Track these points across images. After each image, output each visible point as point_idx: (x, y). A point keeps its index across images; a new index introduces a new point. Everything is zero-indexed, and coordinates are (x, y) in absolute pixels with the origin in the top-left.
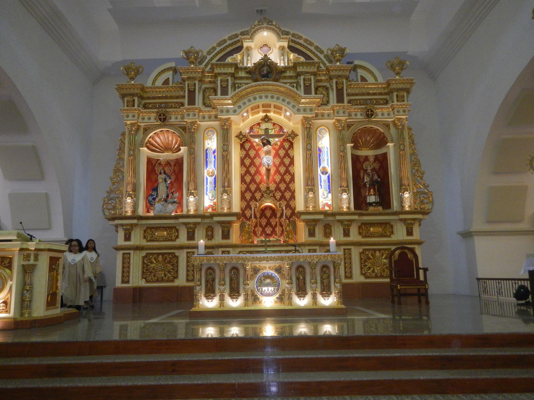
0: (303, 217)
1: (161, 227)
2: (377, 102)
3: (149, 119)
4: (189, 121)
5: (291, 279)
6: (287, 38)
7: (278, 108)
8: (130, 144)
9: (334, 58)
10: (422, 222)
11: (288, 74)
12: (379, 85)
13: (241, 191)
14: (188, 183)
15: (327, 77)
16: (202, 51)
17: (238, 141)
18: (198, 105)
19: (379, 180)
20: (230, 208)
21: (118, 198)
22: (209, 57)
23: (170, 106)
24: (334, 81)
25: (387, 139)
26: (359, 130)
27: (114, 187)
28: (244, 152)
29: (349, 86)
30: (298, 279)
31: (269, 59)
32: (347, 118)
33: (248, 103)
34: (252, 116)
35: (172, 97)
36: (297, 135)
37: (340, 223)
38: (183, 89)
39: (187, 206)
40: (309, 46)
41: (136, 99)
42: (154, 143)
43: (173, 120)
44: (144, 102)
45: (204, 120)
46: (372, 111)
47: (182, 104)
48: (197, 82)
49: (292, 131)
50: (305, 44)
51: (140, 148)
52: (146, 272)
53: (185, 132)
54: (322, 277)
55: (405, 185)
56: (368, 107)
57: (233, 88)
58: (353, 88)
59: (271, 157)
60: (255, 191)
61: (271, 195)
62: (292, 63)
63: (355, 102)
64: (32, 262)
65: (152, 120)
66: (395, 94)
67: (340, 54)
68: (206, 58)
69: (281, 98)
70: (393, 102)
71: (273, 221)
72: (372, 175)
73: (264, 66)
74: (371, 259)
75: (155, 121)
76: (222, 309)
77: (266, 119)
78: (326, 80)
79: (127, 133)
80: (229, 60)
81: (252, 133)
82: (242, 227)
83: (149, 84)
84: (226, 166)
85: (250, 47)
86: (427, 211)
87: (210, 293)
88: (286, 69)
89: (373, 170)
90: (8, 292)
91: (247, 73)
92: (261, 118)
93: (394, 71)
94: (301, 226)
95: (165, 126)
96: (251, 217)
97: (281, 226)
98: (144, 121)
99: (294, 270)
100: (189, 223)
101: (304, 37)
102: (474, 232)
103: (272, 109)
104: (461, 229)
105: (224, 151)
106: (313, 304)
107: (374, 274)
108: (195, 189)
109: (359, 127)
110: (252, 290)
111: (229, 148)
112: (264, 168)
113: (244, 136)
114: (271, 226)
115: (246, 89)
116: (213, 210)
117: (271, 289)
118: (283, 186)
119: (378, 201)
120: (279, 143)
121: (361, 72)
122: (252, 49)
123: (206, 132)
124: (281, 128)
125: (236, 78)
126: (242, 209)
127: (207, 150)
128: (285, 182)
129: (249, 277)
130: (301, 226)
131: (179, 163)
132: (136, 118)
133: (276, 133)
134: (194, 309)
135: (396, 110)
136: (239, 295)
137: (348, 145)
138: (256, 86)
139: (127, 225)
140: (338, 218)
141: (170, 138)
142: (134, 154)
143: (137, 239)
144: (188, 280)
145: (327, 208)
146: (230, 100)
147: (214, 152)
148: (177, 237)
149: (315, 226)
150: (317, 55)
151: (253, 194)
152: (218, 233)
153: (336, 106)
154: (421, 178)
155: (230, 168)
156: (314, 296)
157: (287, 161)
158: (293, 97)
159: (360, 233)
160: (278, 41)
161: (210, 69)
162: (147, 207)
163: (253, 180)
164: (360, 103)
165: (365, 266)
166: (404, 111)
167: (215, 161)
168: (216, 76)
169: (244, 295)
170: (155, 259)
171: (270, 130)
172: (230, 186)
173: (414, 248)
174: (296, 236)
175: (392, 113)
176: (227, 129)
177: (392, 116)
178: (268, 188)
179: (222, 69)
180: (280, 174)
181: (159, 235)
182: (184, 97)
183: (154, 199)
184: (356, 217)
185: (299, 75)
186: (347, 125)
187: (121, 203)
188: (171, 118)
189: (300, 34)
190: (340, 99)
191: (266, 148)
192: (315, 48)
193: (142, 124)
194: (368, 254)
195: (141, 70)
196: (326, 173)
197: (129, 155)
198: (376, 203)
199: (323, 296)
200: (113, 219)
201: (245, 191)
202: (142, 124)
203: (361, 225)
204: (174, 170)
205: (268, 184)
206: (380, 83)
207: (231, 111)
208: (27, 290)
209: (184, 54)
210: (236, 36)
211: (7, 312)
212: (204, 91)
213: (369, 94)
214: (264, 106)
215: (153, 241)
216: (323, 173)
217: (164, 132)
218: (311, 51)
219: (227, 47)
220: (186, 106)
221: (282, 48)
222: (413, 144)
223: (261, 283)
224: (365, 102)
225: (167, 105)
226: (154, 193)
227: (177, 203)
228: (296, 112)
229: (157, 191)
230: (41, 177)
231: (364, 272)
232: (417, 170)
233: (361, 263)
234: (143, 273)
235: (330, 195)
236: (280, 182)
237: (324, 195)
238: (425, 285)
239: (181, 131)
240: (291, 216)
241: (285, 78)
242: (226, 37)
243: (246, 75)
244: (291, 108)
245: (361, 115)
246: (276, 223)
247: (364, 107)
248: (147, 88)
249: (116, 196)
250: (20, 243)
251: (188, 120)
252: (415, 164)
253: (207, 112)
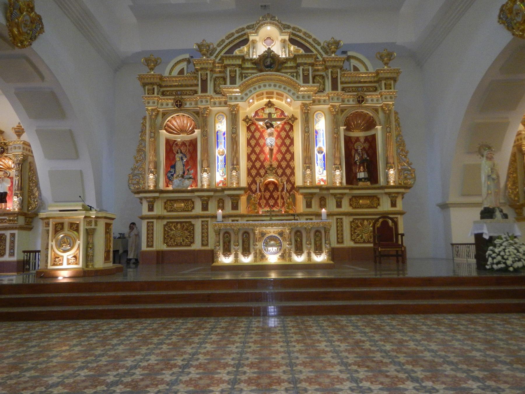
0: (301, 191)
1: (179, 200)
2: (367, 89)
3: (167, 105)
4: (203, 107)
5: (291, 241)
6: (288, 32)
7: (280, 96)
8: (151, 126)
9: (330, 49)
10: (405, 196)
11: (289, 64)
12: (369, 74)
13: (248, 168)
14: (202, 161)
15: (323, 67)
16: (212, 44)
17: (244, 123)
18: (210, 93)
19: (368, 158)
20: (238, 183)
21: (141, 174)
22: (219, 49)
23: (185, 93)
24: (330, 70)
25: (375, 122)
26: (351, 114)
27: (139, 164)
28: (250, 134)
29: (343, 76)
30: (296, 241)
31: (273, 51)
32: (341, 104)
33: (253, 91)
34: (257, 101)
35: (187, 86)
36: (297, 119)
37: (333, 196)
38: (196, 78)
39: (202, 182)
40: (308, 39)
41: (156, 87)
42: (171, 125)
43: (188, 105)
44: (162, 89)
45: (215, 106)
46: (362, 97)
47: (196, 92)
48: (208, 72)
49: (293, 115)
50: (304, 37)
51: (160, 131)
52: (167, 238)
53: (199, 117)
54: (315, 240)
55: (390, 163)
56: (360, 94)
57: (240, 77)
58: (346, 76)
59: (273, 139)
60: (260, 168)
61: (274, 171)
62: (292, 54)
63: (348, 89)
64: (93, 227)
65: (170, 106)
66: (383, 82)
67: (336, 47)
68: (216, 50)
69: (283, 86)
70: (381, 89)
71: (275, 195)
72: (362, 154)
73: (267, 57)
74: (360, 227)
75: (173, 107)
76: (236, 264)
77: (270, 104)
78: (322, 70)
79: (148, 118)
80: (237, 52)
81: (257, 117)
82: (249, 199)
83: (166, 74)
84: (235, 147)
85: (256, 40)
86: (409, 186)
87: (227, 251)
88: (287, 60)
89: (364, 149)
90: (77, 249)
91: (253, 63)
92: (265, 103)
93: (383, 61)
94: (300, 199)
95: (181, 111)
96: (256, 191)
97: (282, 198)
98: (162, 107)
99: (293, 234)
100: (203, 196)
101: (303, 30)
102: (451, 204)
103: (275, 95)
104: (440, 201)
105: (233, 133)
106: (308, 260)
107: (363, 240)
108: (208, 167)
109: (351, 111)
110: (260, 250)
111: (238, 131)
112: (268, 148)
113: (250, 120)
114: (274, 198)
115: (251, 78)
116: (223, 184)
117: (275, 249)
118: (284, 164)
119: (367, 177)
120: (281, 126)
121: (353, 62)
122: (257, 41)
123: (217, 116)
124: (283, 113)
125: (243, 69)
126: (248, 183)
127: (217, 132)
128: (286, 160)
129: (258, 239)
130: (300, 199)
131: (193, 143)
132: (156, 104)
133: (279, 117)
134: (214, 264)
135: (384, 97)
136: (250, 253)
137: (341, 127)
138: (260, 76)
139: (150, 197)
140: (332, 191)
141: (185, 122)
142: (155, 136)
143: (159, 210)
144: (203, 245)
145: (322, 183)
146: (237, 88)
147: (224, 134)
148: (193, 208)
149: (312, 198)
150: (314, 46)
151: (258, 170)
152: (228, 204)
153: (331, 93)
154: (405, 157)
155: (238, 148)
156: (309, 255)
157: (288, 142)
158: (293, 86)
159: (351, 205)
160: (281, 35)
161: (219, 60)
162: (166, 182)
163: (258, 159)
164: (352, 90)
165: (355, 233)
166: (391, 98)
167: (225, 142)
168: (225, 67)
169: (254, 254)
170: (175, 227)
171: (273, 114)
172: (238, 164)
173: (397, 218)
174: (295, 207)
175: (380, 99)
176: (236, 114)
177: (381, 102)
178: (271, 165)
179: (231, 61)
180: (282, 153)
181: (177, 206)
182: (197, 85)
183: (172, 175)
184: (347, 191)
185: (298, 65)
186: (341, 109)
187: (144, 179)
188: (186, 104)
189: (300, 28)
190: (334, 87)
191: (269, 131)
192: (313, 40)
193: (161, 110)
194: (357, 223)
195: (159, 61)
196: (322, 152)
197: (151, 137)
198: (365, 179)
199: (316, 254)
200: (138, 193)
201: (251, 168)
202: (161, 110)
203: (352, 198)
204: (189, 150)
205: (271, 162)
206: (370, 73)
207: (239, 98)
208: (91, 248)
209: (197, 47)
210: (243, 29)
211: (76, 264)
212: (215, 80)
213: (360, 82)
214: (267, 93)
215: (172, 211)
216: (319, 153)
217: (180, 117)
218: (309, 43)
219: (235, 39)
220: (200, 93)
221: (284, 41)
222: (399, 126)
223: (267, 244)
224: (356, 89)
225: (182, 93)
226: (172, 170)
227: (192, 179)
228: (296, 99)
229: (175, 168)
230: (76, 156)
231: (353, 238)
232: (402, 150)
233: (351, 231)
234: (165, 238)
235: (325, 172)
236: (282, 160)
237: (320, 172)
238: (402, 248)
239: (196, 115)
240: (291, 190)
241: (286, 68)
242: (234, 31)
243: (253, 66)
244: (292, 96)
245: (353, 101)
246: (278, 196)
247: (356, 93)
248: (165, 77)
249: (139, 172)
250: (84, 212)
251: (202, 106)
252: (400, 145)
253: (217, 98)
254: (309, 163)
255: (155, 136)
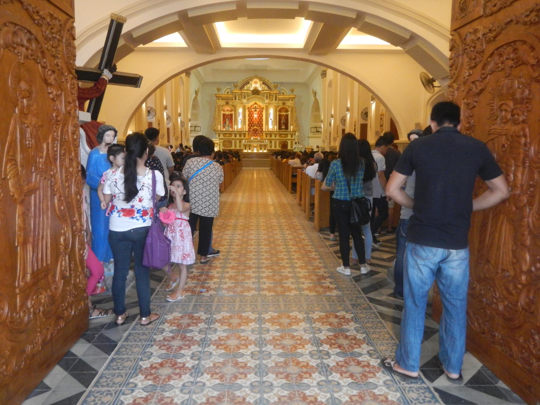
43: (230, 104)
47: (232, 100)
52: (224, 145)
77: (256, 103)
80: (245, 88)
87: (245, 149)
121: (282, 91)
131: (231, 115)
143: (222, 136)
190: (276, 100)
221: (260, 84)
251: (235, 104)
254: (267, 123)
255: (219, 113)
